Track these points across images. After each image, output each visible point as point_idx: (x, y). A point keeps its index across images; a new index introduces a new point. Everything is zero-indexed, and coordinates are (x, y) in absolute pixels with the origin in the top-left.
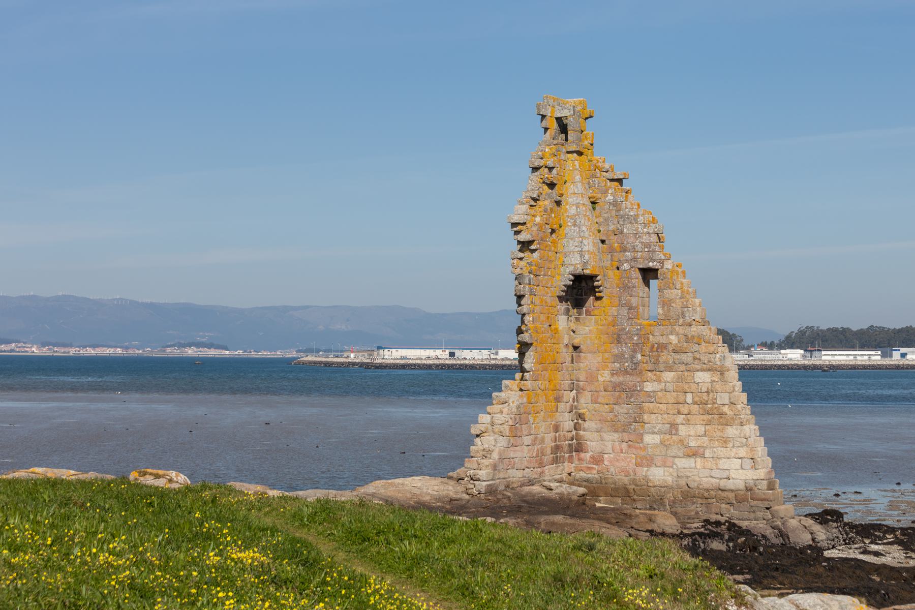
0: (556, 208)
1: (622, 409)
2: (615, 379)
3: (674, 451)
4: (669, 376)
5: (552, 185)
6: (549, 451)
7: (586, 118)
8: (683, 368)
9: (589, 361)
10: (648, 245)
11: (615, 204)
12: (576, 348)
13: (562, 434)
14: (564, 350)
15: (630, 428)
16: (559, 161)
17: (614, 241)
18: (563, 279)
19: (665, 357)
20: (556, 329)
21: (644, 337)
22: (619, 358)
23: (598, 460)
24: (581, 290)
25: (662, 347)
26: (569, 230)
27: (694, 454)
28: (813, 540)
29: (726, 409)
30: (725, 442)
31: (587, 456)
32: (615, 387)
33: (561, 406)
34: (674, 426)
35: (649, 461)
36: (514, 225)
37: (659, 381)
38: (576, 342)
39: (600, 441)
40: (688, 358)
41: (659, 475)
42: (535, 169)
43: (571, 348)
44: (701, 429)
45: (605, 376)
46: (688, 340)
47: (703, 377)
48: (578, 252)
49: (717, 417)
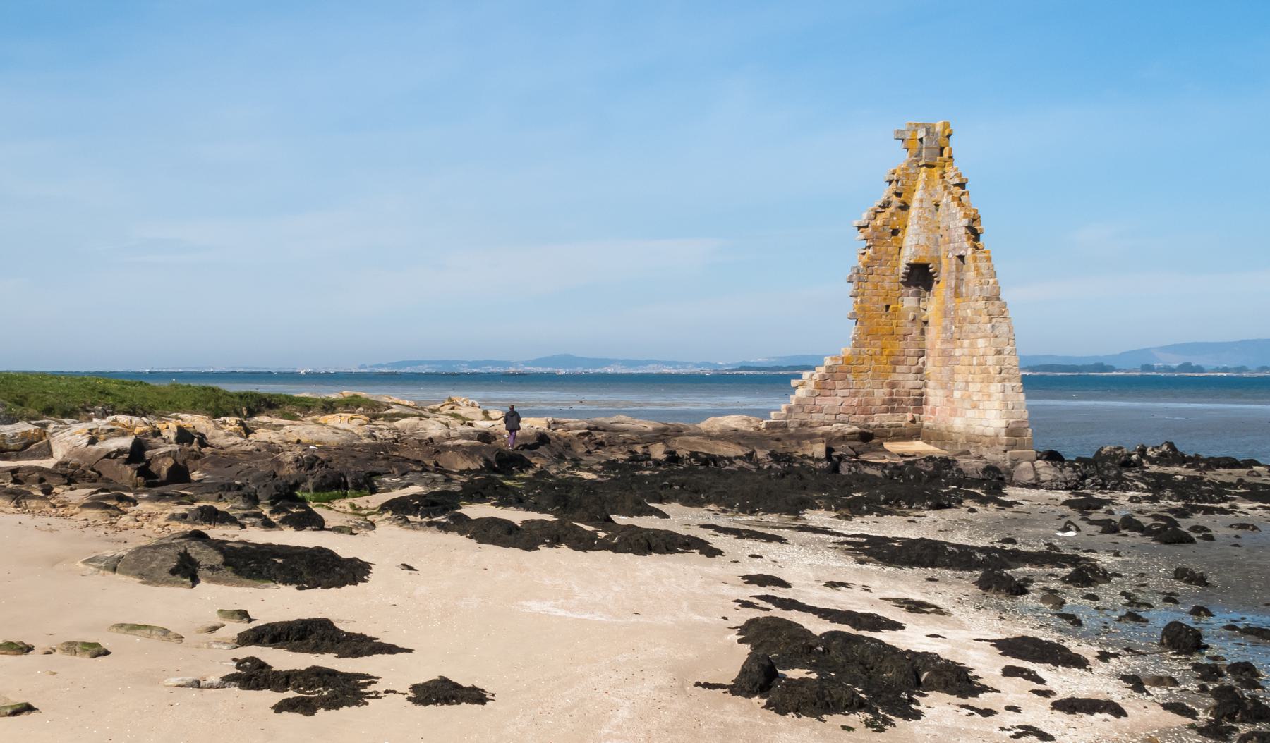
0: (901, 213)
1: (946, 370)
2: (944, 347)
3: (967, 405)
4: (966, 343)
5: (898, 195)
6: (878, 402)
7: (949, 136)
8: (972, 336)
9: (932, 332)
10: (960, 236)
11: (947, 205)
12: (926, 323)
13: (901, 390)
14: (909, 325)
15: (947, 385)
16: (907, 176)
17: (945, 233)
18: (902, 268)
19: (967, 327)
20: (896, 309)
21: (956, 311)
22: (945, 329)
23: (933, 412)
24: (920, 276)
25: (964, 319)
26: (910, 230)
27: (975, 407)
28: (1038, 479)
29: (991, 370)
30: (990, 395)
31: (929, 408)
32: (944, 351)
33: (899, 368)
34: (967, 382)
35: (954, 413)
36: (859, 228)
37: (961, 347)
38: (924, 318)
39: (935, 396)
40: (974, 327)
41: (958, 424)
42: (890, 182)
43: (919, 324)
44: (979, 385)
45: (938, 345)
46: (977, 312)
47: (981, 343)
48: (911, 248)
49: (988, 379)
